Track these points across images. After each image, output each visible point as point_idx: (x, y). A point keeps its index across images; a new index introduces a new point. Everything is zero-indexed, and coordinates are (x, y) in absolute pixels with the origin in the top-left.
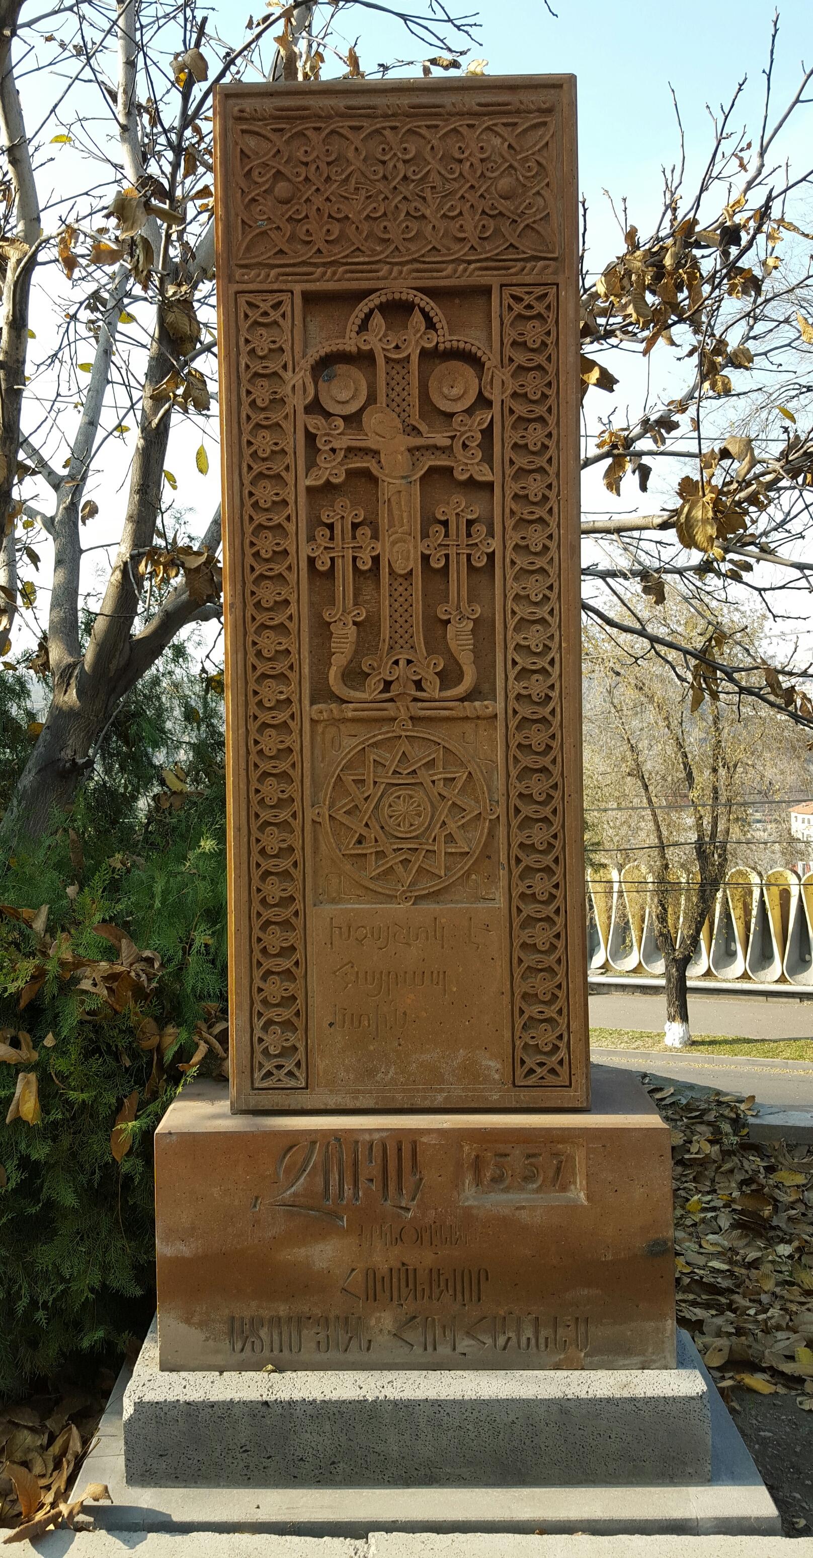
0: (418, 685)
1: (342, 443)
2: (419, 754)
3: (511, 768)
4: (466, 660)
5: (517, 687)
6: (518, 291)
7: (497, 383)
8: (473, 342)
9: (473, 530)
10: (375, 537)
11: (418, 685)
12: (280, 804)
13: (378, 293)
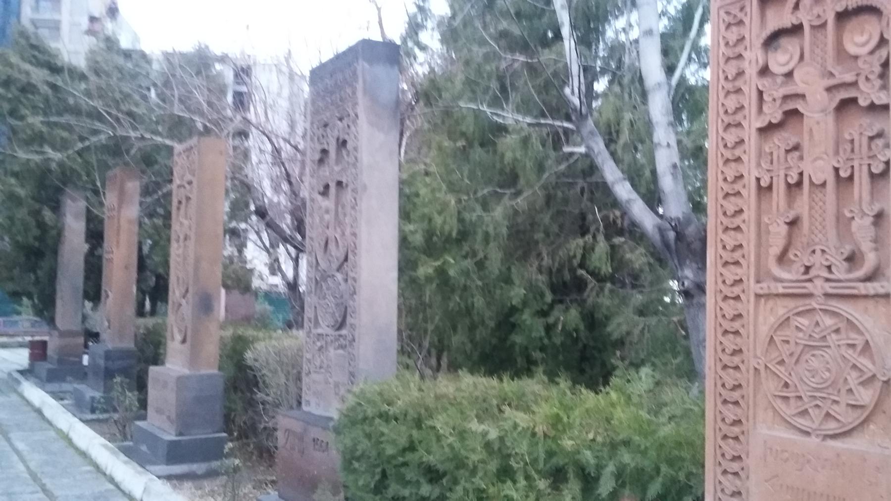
0: (829, 268)
2: (828, 321)
4: (866, 246)
11: (829, 268)
12: (735, 352)
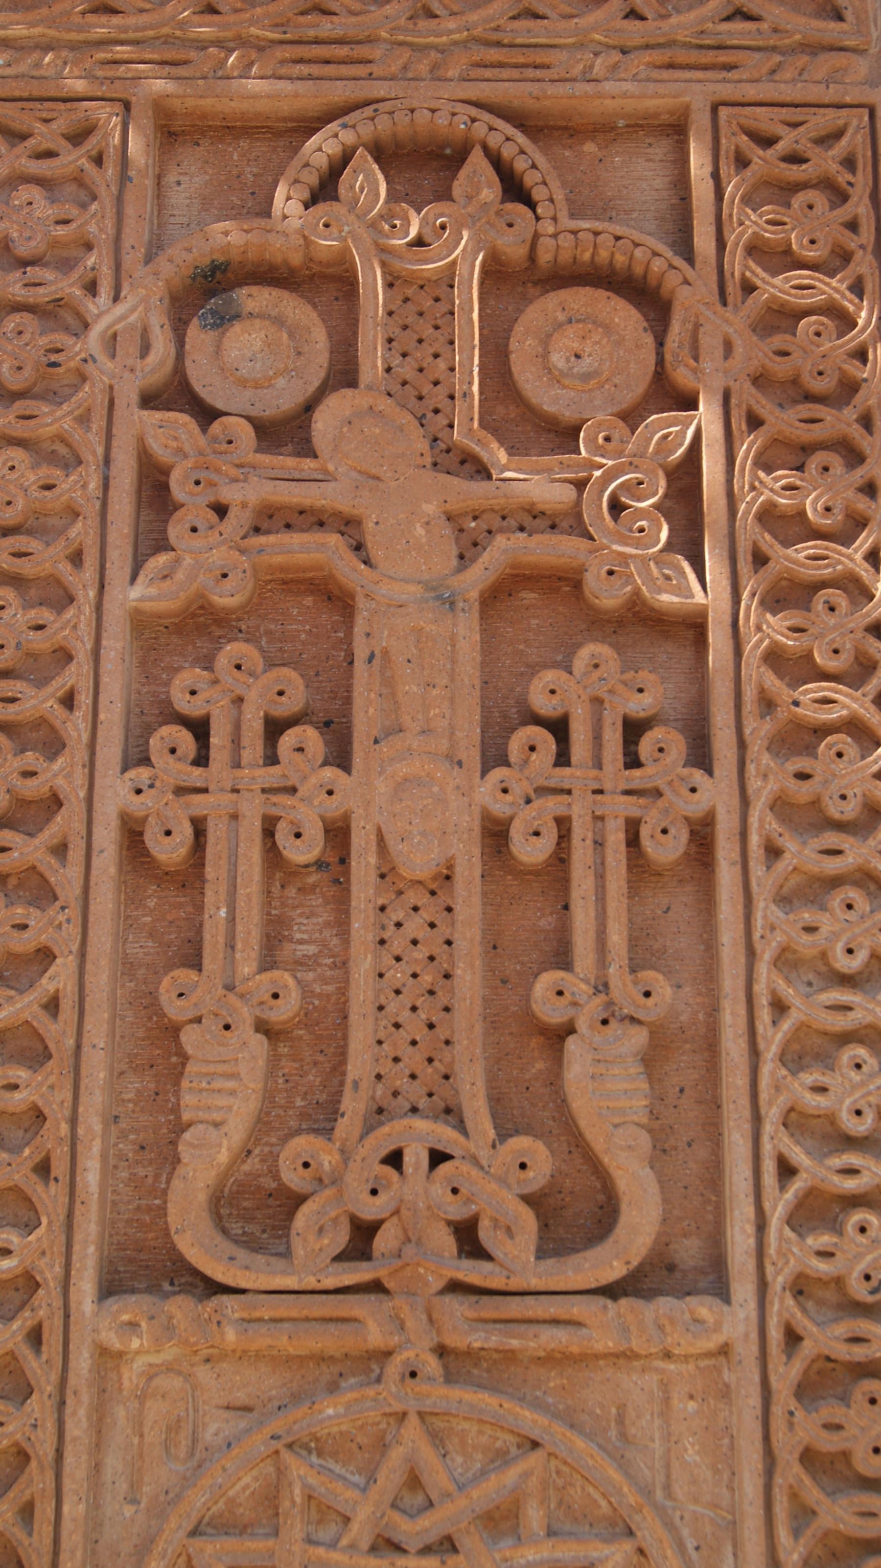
1: (246, 494)
3: (783, 1534)
5: (795, 1253)
6: (764, 119)
7: (710, 343)
8: (637, 236)
9: (646, 747)
10: (341, 757)
13: (368, 111)
